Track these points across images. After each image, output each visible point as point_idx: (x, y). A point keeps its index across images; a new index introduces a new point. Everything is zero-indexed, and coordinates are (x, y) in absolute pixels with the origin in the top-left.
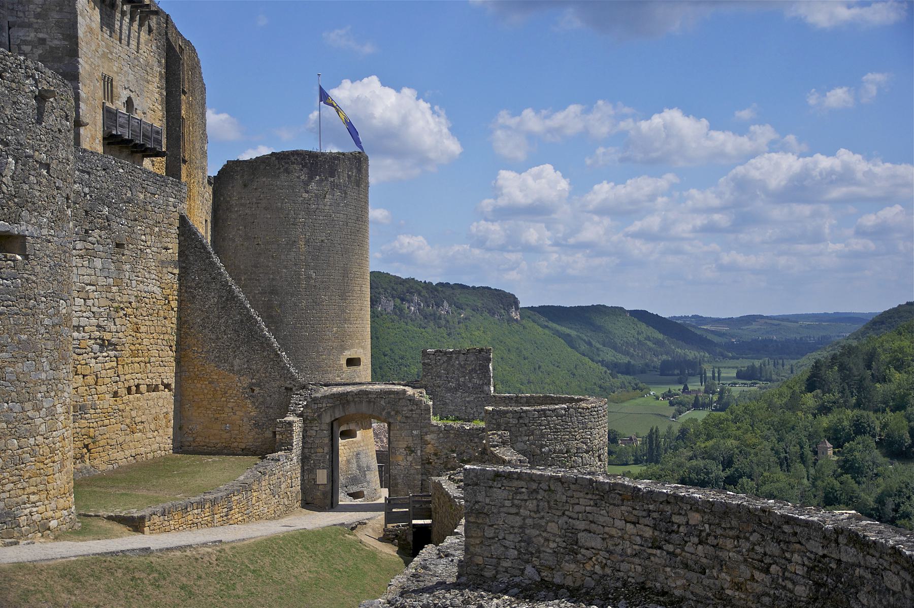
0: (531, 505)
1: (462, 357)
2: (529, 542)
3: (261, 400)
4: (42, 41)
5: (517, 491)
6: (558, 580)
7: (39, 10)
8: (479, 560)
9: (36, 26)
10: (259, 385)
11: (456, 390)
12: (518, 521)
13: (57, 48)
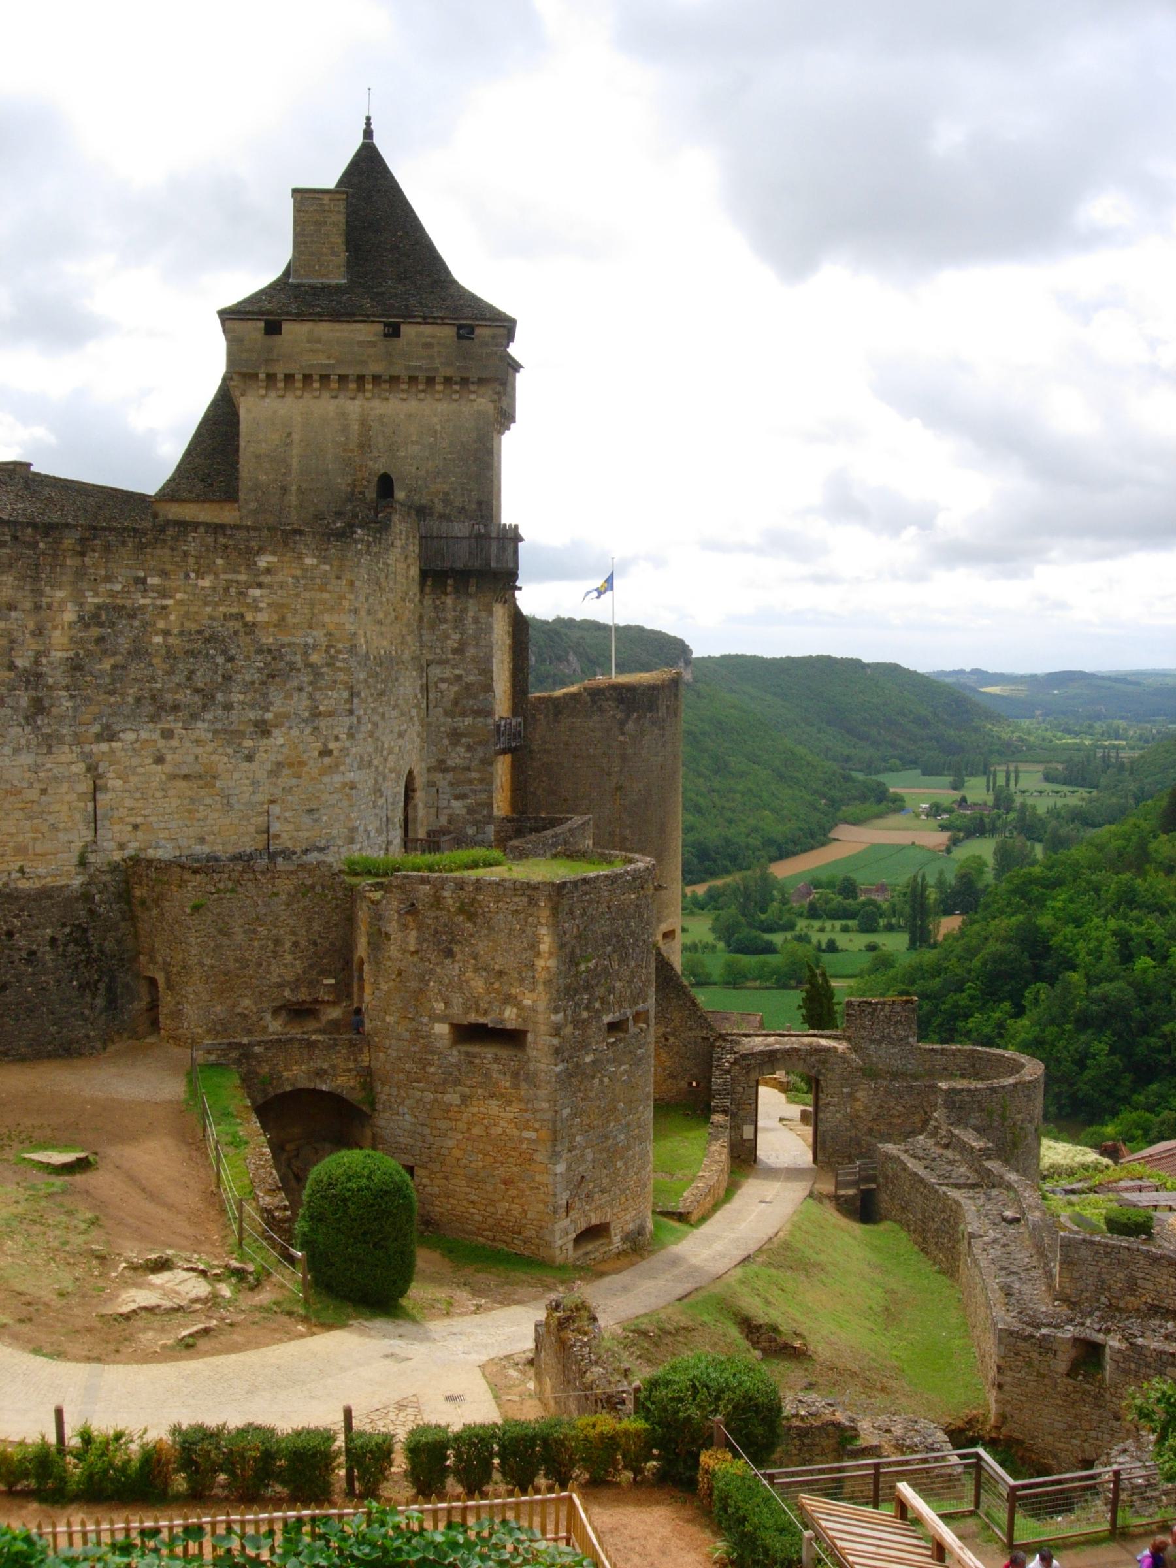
0: (1107, 1260)
1: (887, 1009)
2: (1103, 1282)
3: (675, 1049)
4: (459, 678)
5: (1097, 1252)
6: (1121, 1305)
7: (456, 645)
8: (1068, 1291)
9: (453, 662)
10: (673, 1035)
11: (879, 1042)
12: (1097, 1270)
13: (473, 684)
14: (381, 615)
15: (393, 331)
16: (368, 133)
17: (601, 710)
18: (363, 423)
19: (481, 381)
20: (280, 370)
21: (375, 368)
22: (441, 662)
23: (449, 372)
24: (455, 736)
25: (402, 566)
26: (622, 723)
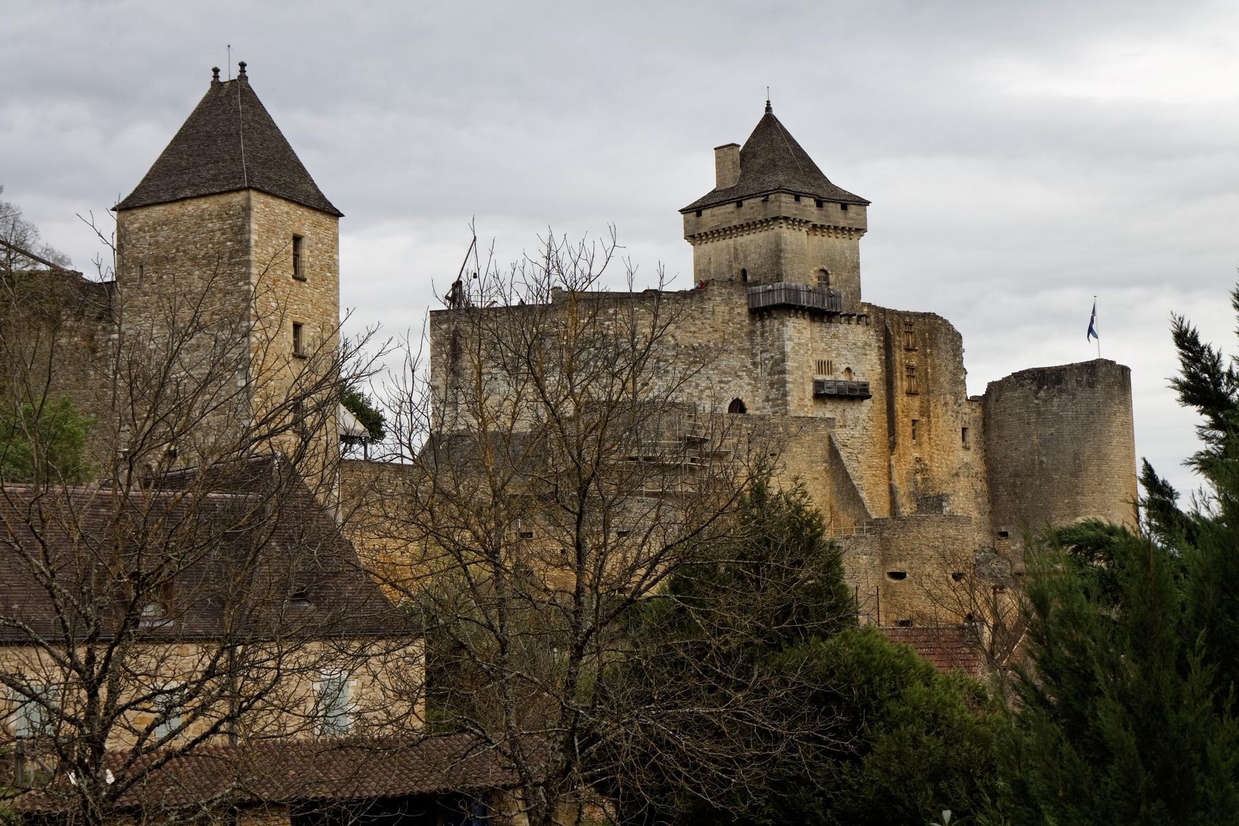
14: (693, 329)
15: (739, 205)
16: (768, 109)
17: (1022, 385)
18: (736, 249)
19: (775, 219)
20: (702, 231)
21: (735, 223)
22: (766, 351)
23: (760, 218)
24: (772, 384)
25: (722, 309)
26: (1036, 393)
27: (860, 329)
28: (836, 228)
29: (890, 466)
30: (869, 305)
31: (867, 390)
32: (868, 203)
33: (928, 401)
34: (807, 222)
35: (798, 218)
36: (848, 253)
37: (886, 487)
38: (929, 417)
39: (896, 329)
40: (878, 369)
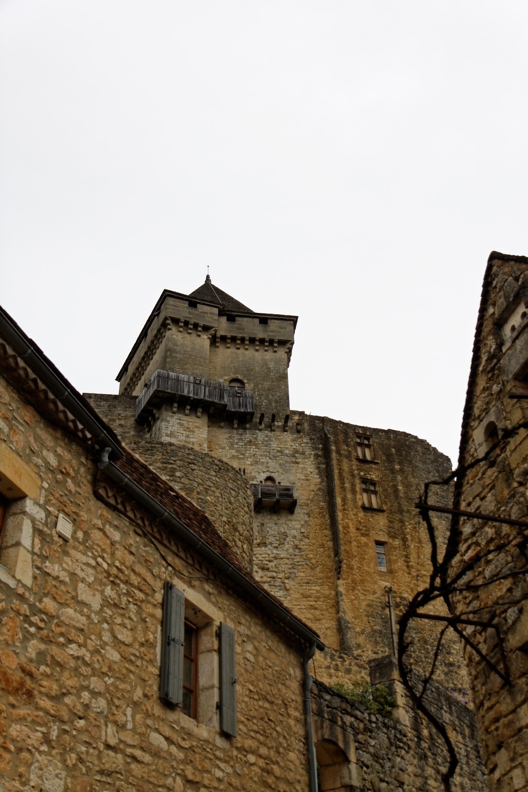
27: (288, 437)
28: (252, 341)
29: (338, 594)
30: (302, 414)
31: (291, 496)
32: (293, 320)
33: (402, 521)
34: (206, 329)
35: (192, 321)
36: (272, 365)
37: (333, 624)
38: (404, 540)
39: (341, 437)
40: (316, 479)
